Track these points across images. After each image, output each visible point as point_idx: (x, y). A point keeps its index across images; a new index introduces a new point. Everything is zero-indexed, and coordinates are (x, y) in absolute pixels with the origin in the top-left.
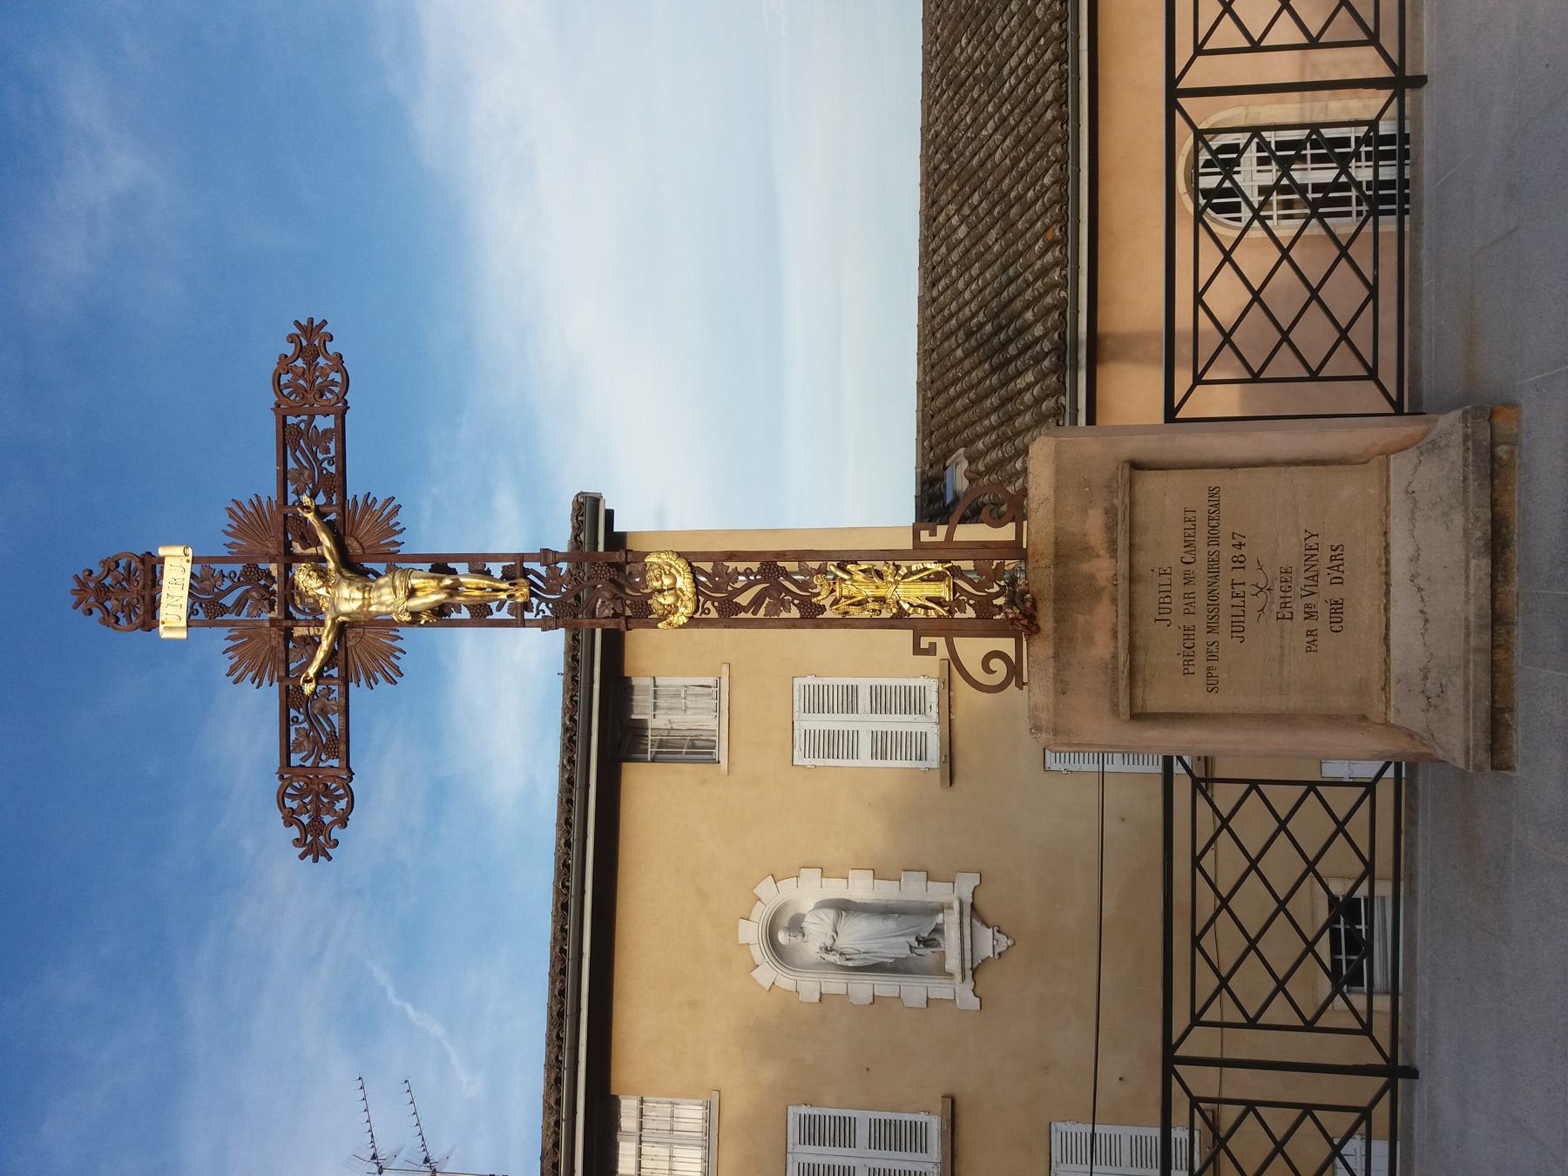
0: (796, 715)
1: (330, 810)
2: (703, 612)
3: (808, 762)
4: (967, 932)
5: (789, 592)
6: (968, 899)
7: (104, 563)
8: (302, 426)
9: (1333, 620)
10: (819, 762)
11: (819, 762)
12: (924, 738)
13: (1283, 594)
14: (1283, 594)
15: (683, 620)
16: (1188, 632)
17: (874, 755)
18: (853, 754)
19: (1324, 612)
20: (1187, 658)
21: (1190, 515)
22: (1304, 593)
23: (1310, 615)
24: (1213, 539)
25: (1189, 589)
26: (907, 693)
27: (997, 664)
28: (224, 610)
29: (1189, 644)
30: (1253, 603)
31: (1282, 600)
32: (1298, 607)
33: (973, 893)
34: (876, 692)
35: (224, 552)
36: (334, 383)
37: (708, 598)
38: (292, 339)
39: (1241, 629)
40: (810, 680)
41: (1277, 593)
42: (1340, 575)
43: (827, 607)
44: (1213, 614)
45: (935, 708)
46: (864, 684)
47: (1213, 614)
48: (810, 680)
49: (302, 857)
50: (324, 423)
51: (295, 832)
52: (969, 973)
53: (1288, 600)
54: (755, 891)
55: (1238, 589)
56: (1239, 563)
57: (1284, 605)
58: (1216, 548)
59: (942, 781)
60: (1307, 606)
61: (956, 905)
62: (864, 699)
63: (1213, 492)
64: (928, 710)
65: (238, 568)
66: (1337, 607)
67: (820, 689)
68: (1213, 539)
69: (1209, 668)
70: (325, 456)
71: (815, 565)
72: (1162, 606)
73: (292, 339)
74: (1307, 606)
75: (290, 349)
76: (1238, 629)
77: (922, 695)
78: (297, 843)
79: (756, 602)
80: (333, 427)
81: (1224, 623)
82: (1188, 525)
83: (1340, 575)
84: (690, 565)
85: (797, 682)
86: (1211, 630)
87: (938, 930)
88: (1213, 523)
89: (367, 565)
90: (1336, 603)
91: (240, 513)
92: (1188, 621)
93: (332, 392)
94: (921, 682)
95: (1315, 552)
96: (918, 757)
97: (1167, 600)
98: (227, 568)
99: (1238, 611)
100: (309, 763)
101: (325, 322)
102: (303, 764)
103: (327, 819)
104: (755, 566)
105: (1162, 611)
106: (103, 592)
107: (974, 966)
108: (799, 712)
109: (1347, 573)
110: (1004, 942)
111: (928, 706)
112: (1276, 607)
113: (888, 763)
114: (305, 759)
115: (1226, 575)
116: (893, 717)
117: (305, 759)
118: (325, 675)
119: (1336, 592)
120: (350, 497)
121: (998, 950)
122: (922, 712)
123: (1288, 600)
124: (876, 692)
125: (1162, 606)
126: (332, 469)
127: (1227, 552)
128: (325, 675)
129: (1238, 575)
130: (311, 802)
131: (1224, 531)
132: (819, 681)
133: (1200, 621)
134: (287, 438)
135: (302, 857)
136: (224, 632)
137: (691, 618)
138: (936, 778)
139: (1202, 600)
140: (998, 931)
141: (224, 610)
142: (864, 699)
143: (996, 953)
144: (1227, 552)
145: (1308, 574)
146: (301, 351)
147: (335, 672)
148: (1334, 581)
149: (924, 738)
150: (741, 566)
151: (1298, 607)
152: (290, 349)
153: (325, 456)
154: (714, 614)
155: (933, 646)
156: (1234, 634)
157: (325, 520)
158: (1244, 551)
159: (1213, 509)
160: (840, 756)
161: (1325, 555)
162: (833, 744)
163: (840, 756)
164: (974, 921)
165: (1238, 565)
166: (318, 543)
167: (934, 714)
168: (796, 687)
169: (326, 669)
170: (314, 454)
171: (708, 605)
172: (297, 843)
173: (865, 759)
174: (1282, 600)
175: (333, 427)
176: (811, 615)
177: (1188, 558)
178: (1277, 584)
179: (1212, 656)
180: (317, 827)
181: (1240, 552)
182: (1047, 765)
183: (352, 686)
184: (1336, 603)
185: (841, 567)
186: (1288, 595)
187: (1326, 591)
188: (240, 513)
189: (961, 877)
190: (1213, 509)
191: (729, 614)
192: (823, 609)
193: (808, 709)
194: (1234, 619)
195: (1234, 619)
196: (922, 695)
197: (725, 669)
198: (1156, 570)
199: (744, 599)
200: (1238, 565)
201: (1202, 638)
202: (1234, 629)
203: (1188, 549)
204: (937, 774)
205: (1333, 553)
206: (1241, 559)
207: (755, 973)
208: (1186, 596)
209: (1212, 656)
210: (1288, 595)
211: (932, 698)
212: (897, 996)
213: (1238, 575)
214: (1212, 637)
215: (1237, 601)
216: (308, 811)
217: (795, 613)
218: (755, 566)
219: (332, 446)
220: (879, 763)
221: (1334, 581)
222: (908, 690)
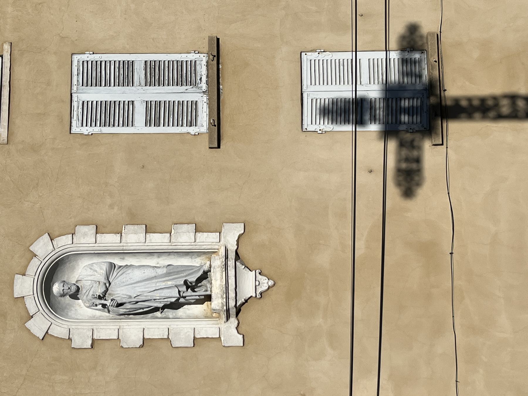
0: (75, 88)
3: (86, 130)
4: (231, 273)
6: (232, 247)
11: (96, 130)
17: (148, 123)
18: (128, 122)
26: (180, 68)
33: (238, 241)
40: (87, 57)
45: (204, 79)
46: (139, 59)
48: (87, 57)
52: (233, 311)
54: (31, 248)
59: (210, 141)
61: (222, 252)
62: (139, 73)
64: (198, 81)
67: (97, 64)
77: (193, 68)
85: (76, 58)
94: (192, 57)
96: (189, 124)
107: (238, 304)
108: (78, 85)
110: (265, 283)
111: (199, 78)
113: (161, 129)
116: (166, 89)
121: (259, 290)
122: (194, 83)
132: (97, 57)
138: (205, 142)
140: (260, 273)
142: (139, 73)
143: (258, 293)
160: (116, 124)
163: (116, 124)
164: (238, 263)
167: (204, 86)
168: (75, 63)
182: (305, 127)
189: (227, 227)
193: (86, 83)
196: (193, 68)
197: (7, 47)
204: (206, 138)
207: (30, 324)
211: (202, 71)
212: (166, 337)
220: (153, 130)
222: (180, 64)
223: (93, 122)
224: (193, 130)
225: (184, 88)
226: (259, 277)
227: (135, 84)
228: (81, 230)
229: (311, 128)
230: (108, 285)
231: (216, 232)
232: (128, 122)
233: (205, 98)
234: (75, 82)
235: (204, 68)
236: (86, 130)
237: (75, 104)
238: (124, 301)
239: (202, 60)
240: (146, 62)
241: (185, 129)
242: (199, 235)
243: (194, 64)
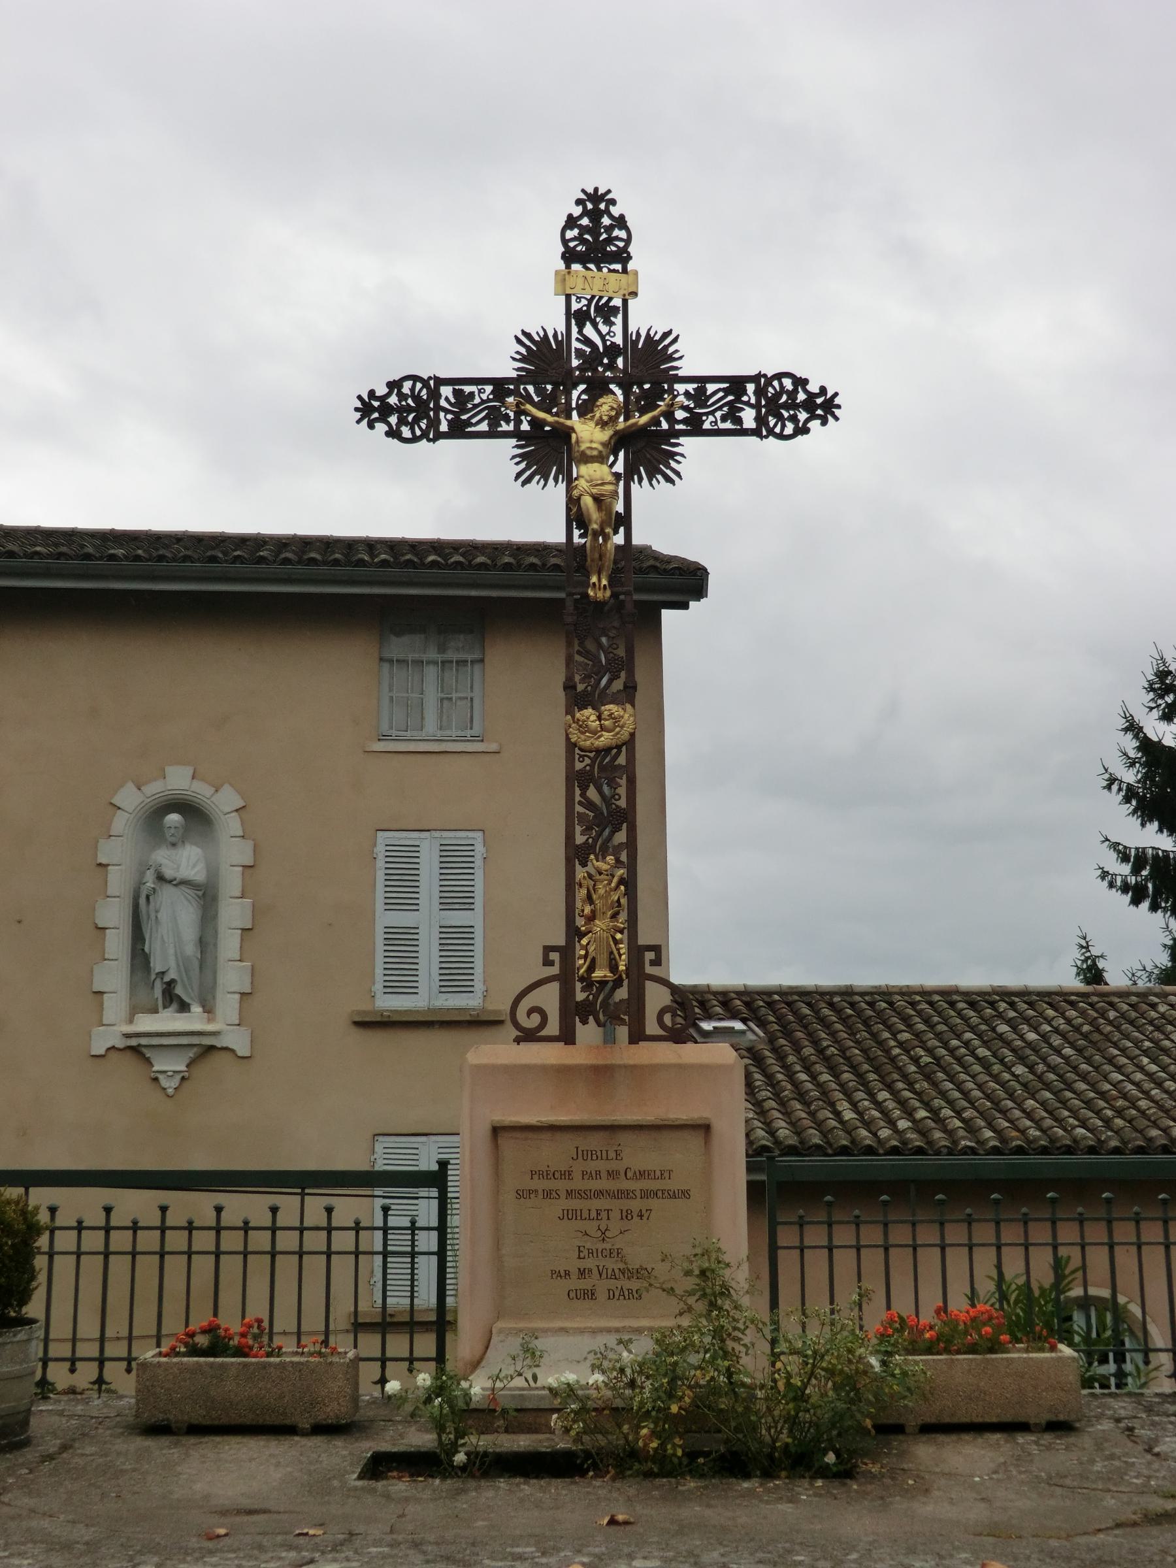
0: (437, 834)
1: (402, 421)
2: (581, 756)
3: (380, 849)
5: (599, 834)
7: (622, 217)
8: (745, 398)
9: (578, 1292)
10: (381, 864)
11: (381, 864)
13: (600, 1251)
14: (600, 1251)
15: (574, 739)
16: (567, 1175)
18: (391, 905)
19: (585, 1284)
20: (545, 1174)
21: (666, 1175)
22: (601, 1268)
23: (582, 1273)
24: (646, 1194)
25: (604, 1175)
27: (536, 1019)
28: (581, 327)
30: (591, 1227)
31: (595, 1251)
32: (590, 1263)
33: (226, 1049)
35: (632, 328)
36: (783, 426)
37: (593, 760)
38: (823, 390)
39: (570, 1217)
40: (479, 848)
41: (600, 1246)
42: (617, 1297)
43: (586, 869)
48: (479, 848)
49: (360, 398)
50: (748, 417)
51: (381, 391)
52: (133, 1042)
53: (595, 1255)
55: (604, 1215)
56: (626, 1215)
57: (590, 1252)
58: (639, 1196)
60: (590, 1271)
62: (457, 918)
63: (685, 1194)
65: (618, 340)
66: (589, 1295)
68: (646, 1194)
69: (536, 1191)
70: (719, 419)
71: (624, 857)
73: (823, 390)
74: (590, 1271)
75: (813, 388)
76: (569, 1215)
78: (372, 393)
79: (589, 805)
80: (745, 426)
81: (575, 1204)
82: (658, 1174)
83: (617, 1297)
84: (623, 744)
85: (479, 835)
86: (569, 1193)
87: (184, 1007)
88: (660, 1194)
89: (621, 454)
91: (666, 342)
92: (577, 1175)
93: (775, 425)
94: (479, 986)
98: (618, 328)
99: (585, 1215)
100: (443, 403)
101: (837, 419)
102: (443, 398)
103: (393, 420)
104: (622, 803)
105: (585, 1153)
106: (595, 215)
109: (618, 1303)
110: (170, 1084)
112: (588, 1245)
114: (447, 399)
115: (616, 1205)
116: (435, 953)
117: (447, 399)
118: (523, 418)
119: (602, 1295)
120: (682, 440)
121: (161, 1077)
123: (595, 1255)
126: (706, 426)
127: (635, 1205)
128: (523, 418)
129: (615, 1215)
130: (408, 404)
131: (654, 1203)
132: (479, 862)
133: (577, 1184)
134: (736, 384)
135: (360, 398)
136: (561, 328)
137: (575, 745)
139: (595, 1185)
140: (183, 1078)
141: (581, 327)
142: (457, 918)
144: (635, 1205)
145: (617, 1271)
146: (811, 396)
147: (525, 427)
148: (611, 1293)
150: (622, 791)
151: (590, 1263)
152: (813, 388)
153: (719, 419)
154: (579, 766)
155: (552, 964)
156: (565, 1212)
157: (662, 419)
158: (636, 1219)
159: (671, 1193)
161: (634, 1285)
164: (195, 1049)
165: (624, 1214)
166: (642, 414)
168: (470, 834)
169: (529, 418)
170: (720, 408)
171: (587, 761)
172: (372, 393)
173: (386, 919)
174: (595, 1251)
175: (745, 426)
176: (576, 854)
177: (630, 1174)
178: (608, 1246)
179: (548, 1194)
180: (386, 411)
181: (635, 1216)
182: (381, 1138)
183: (514, 442)
184: (593, 1294)
185: (621, 881)
186: (600, 1254)
187: (602, 1287)
188: (666, 342)
190: (671, 1193)
191: (577, 780)
192: (584, 865)
193: (445, 850)
197: (493, 747)
198: (619, 1148)
199: (592, 793)
200: (624, 1214)
201: (562, 1185)
202: (570, 1212)
205: (634, 1293)
206: (629, 1217)
208: (598, 1173)
209: (548, 1194)
210: (600, 1254)
213: (615, 1215)
214: (563, 1195)
215: (594, 1214)
216: (400, 402)
217: (580, 839)
218: (622, 803)
219: (728, 425)
221: (611, 1293)
224: (378, 987)
226: (178, 1077)
227: (442, 912)
228: (248, 846)
229: (379, 1148)
230: (174, 883)
231: (240, 1019)
234: (445, 834)
236: (380, 849)
238: (152, 904)
240: (473, 927)
242: (237, 996)
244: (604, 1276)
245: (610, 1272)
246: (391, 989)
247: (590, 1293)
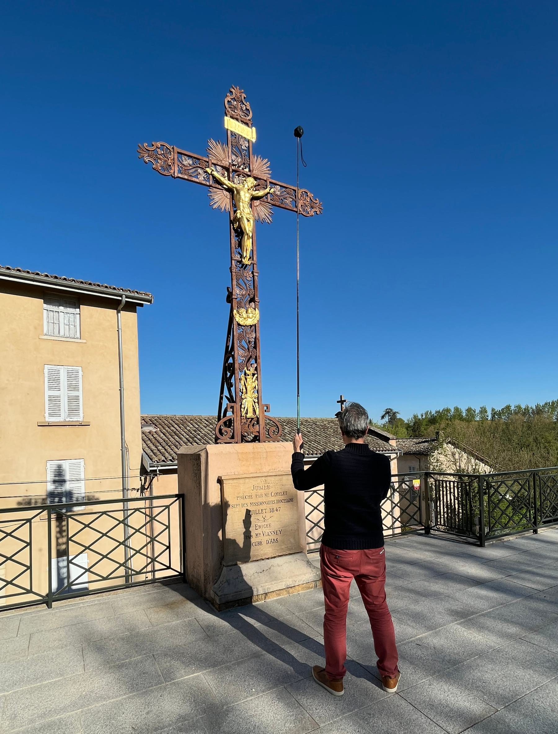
0: (66, 367)
3: (46, 371)
10: (46, 375)
11: (46, 375)
12: (59, 415)
16: (251, 497)
17: (50, 396)
18: (50, 388)
20: (242, 497)
25: (264, 495)
29: (247, 497)
34: (77, 398)
40: (81, 373)
41: (263, 524)
42: (269, 543)
44: (256, 504)
45: (71, 420)
46: (80, 393)
47: (256, 504)
48: (81, 373)
55: (264, 511)
58: (276, 503)
59: (40, 422)
60: (260, 534)
64: (70, 417)
67: (77, 377)
72: (258, 487)
74: (260, 534)
82: (282, 493)
83: (269, 543)
88: (283, 501)
90: (261, 543)
92: (254, 496)
94: (81, 415)
95: (276, 534)
97: (260, 489)
108: (68, 369)
112: (259, 524)
122: (69, 415)
124: (77, 398)
125: (258, 487)
132: (80, 377)
138: (41, 420)
139: (260, 500)
145: (269, 533)
149: (59, 415)
159: (287, 500)
162: (54, 381)
165: (271, 510)
167: (68, 420)
168: (77, 368)
173: (48, 393)
190: (287, 500)
194: (255, 511)
195: (255, 511)
197: (85, 341)
200: (271, 510)
203: (275, 494)
206: (273, 511)
211: (75, 419)
220: (47, 399)
223: (50, 374)
224: (47, 415)
225: (67, 412)
232: (50, 388)
233: (62, 420)
234: (69, 367)
235: (76, 420)
237: (59, 367)
239: (80, 419)
241: (47, 412)
243: (78, 415)
244: (265, 535)
245: (267, 533)
246: (51, 415)
247: (260, 543)
